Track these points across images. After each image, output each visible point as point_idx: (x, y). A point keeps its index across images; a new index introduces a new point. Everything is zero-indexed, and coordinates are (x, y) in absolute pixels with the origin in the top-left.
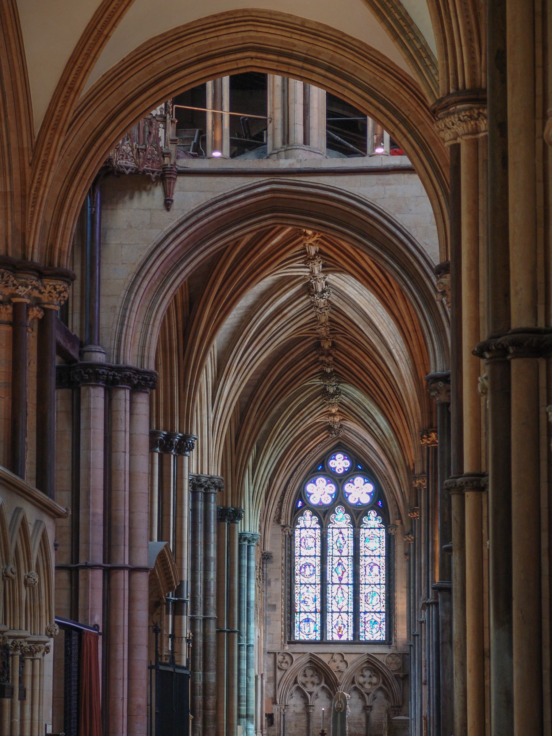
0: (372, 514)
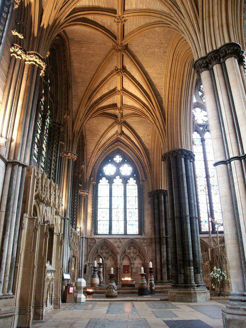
0: (132, 179)
